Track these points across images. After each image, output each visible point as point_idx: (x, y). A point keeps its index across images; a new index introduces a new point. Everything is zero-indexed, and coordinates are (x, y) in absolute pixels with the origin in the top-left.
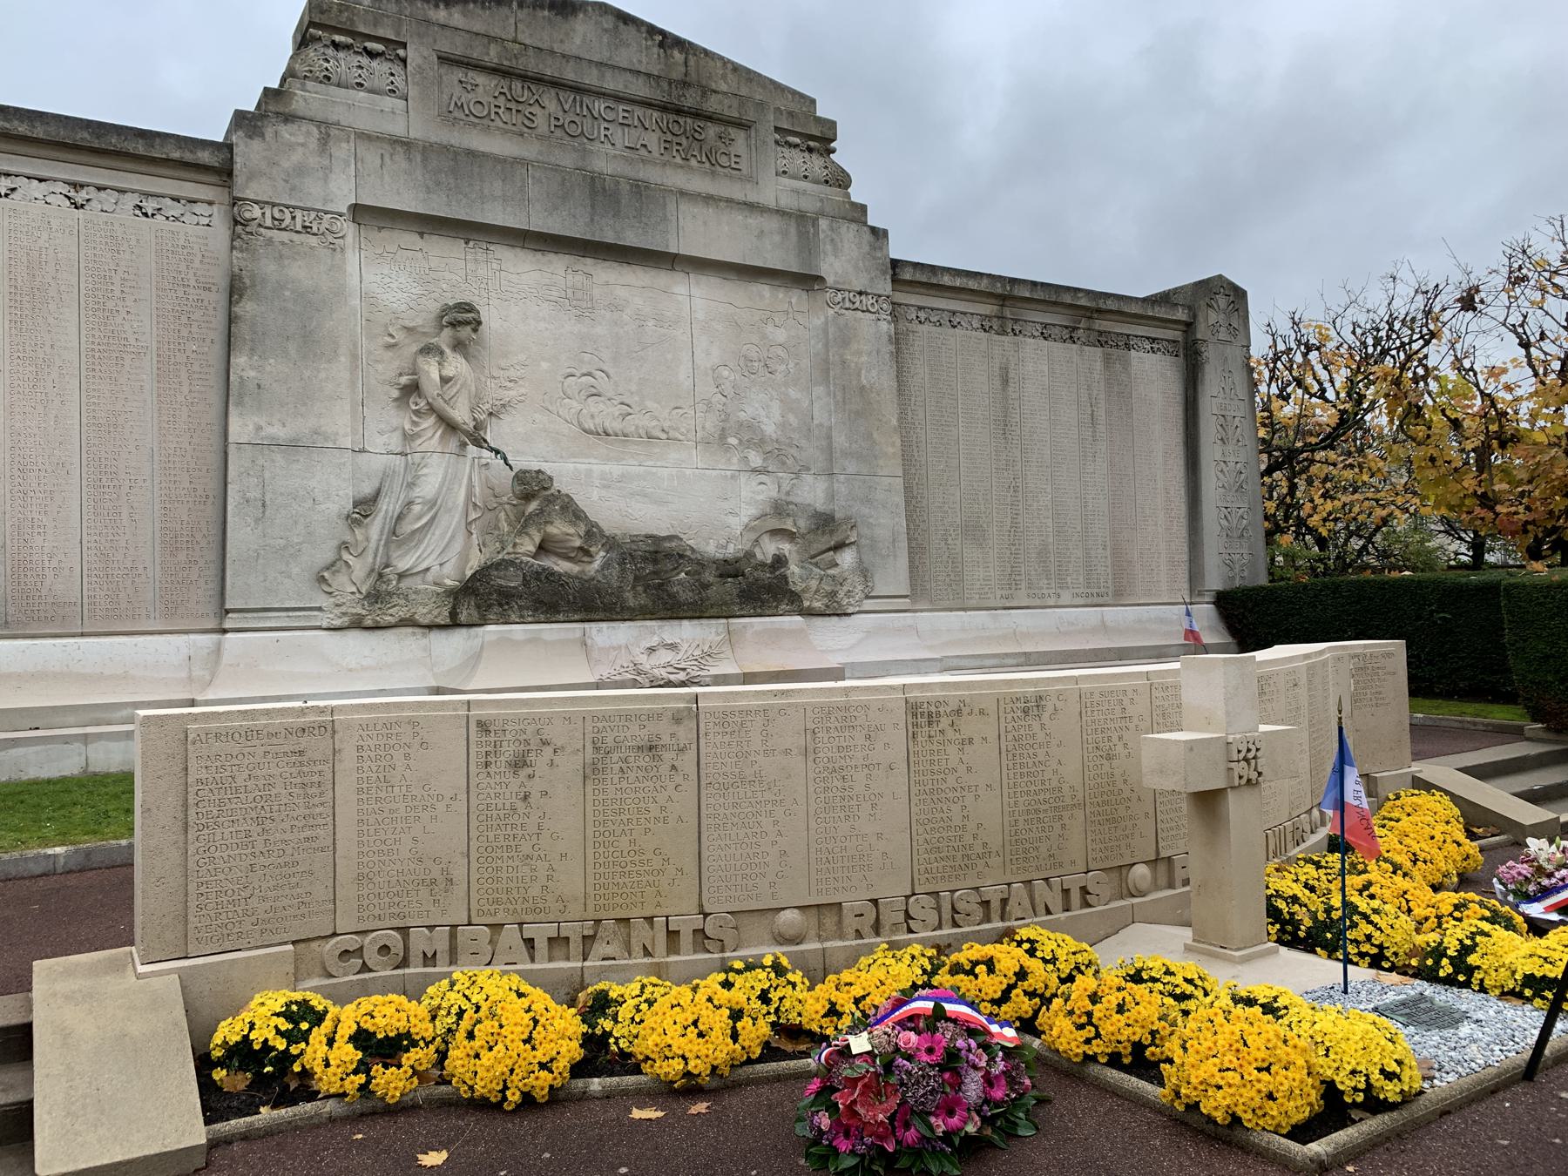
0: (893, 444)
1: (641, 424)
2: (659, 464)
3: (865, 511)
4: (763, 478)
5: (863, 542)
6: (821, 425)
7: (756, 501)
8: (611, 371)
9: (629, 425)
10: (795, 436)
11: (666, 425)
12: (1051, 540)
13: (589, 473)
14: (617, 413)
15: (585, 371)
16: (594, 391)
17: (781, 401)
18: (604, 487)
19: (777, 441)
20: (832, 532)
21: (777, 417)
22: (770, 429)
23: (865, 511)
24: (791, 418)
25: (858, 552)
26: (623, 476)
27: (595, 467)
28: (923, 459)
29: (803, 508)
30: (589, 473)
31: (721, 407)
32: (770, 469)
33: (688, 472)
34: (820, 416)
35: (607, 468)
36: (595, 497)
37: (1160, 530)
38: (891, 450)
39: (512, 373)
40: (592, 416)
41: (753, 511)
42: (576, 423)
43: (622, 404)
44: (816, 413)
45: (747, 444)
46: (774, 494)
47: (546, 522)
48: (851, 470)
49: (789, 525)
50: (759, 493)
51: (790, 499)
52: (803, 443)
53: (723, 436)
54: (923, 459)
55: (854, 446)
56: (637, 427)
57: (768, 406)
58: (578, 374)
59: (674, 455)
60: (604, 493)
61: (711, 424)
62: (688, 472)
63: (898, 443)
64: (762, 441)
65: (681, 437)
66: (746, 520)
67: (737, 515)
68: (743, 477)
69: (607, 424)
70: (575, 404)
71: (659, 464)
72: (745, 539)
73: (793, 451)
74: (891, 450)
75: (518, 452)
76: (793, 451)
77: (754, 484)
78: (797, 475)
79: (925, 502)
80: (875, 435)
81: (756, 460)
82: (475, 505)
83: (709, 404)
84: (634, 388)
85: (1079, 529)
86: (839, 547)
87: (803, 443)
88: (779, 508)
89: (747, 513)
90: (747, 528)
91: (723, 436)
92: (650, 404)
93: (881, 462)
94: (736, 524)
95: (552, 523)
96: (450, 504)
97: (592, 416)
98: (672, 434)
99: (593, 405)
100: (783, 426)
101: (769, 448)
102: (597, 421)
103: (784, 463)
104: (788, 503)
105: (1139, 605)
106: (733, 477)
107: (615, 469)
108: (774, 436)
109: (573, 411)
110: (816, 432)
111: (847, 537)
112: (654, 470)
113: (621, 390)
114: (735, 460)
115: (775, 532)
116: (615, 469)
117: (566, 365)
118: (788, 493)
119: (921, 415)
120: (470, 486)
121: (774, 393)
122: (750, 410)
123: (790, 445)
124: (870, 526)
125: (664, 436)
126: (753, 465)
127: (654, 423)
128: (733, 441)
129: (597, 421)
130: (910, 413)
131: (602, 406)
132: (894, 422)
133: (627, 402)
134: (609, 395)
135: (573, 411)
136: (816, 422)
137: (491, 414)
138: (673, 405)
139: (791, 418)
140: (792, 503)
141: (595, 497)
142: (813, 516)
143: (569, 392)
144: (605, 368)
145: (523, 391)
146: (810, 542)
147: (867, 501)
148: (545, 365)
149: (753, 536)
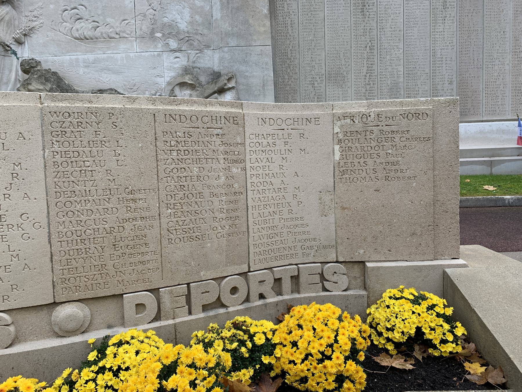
0: (264, 25)
1: (104, 31)
2: (115, 52)
3: (243, 68)
4: (177, 54)
5: (241, 87)
6: (216, 19)
7: (174, 68)
8: (86, 4)
9: (97, 33)
10: (200, 28)
11: (118, 30)
12: (401, 80)
13: (77, 60)
14: (91, 27)
15: (72, 6)
16: (78, 17)
17: (191, 8)
18: (86, 67)
19: (188, 32)
20: (216, 83)
21: (187, 17)
22: (183, 26)
23: (243, 68)
24: (197, 17)
25: (238, 94)
26: (95, 60)
27: (80, 57)
28: (296, 36)
29: (205, 70)
30: (77, 60)
31: (152, 17)
32: (183, 49)
33: (131, 55)
34: (217, 14)
35: (86, 57)
36: (81, 72)
37: (507, 67)
38: (262, 29)
39: (35, 13)
40: (77, 30)
41: (173, 74)
42: (69, 34)
43: (94, 21)
44: (214, 13)
45: (170, 35)
46: (185, 63)
47: (28, 84)
48: (232, 44)
49: (187, 79)
50: (175, 64)
51: (196, 65)
52: (206, 31)
53: (153, 32)
54: (296, 36)
55: (235, 29)
56: (102, 34)
57: (181, 13)
58: (69, 9)
59: (122, 46)
60: (86, 70)
61: (145, 27)
62: (131, 55)
63: (268, 23)
64: (178, 33)
65: (127, 36)
66: (168, 79)
67: (162, 77)
68: (165, 55)
69: (85, 33)
70: (68, 24)
71: (115, 52)
72: (166, 89)
73: (199, 37)
74: (262, 29)
75: (41, 53)
76: (199, 37)
77: (172, 58)
78: (201, 51)
79: (297, 61)
80: (251, 21)
81: (173, 44)
82: (19, 80)
83: (145, 16)
84: (100, 12)
85: (427, 71)
86: (221, 91)
87: (206, 31)
88: (186, 71)
89: (168, 75)
90: (169, 83)
91: (153, 32)
92: (109, 20)
93: (255, 37)
94: (162, 82)
95: (31, 84)
96: (5, 80)
97: (77, 30)
98: (122, 35)
99: (78, 25)
100: (191, 23)
101: (182, 37)
102: (80, 32)
103: (191, 45)
104: (193, 68)
105: (482, 121)
106: (159, 55)
107: (91, 57)
108: (186, 29)
109: (67, 28)
110: (214, 25)
111: (225, 84)
112: (112, 55)
113: (92, 14)
114: (160, 45)
115: (182, 85)
116: (91, 57)
117: (63, 5)
118: (194, 62)
119: (294, 6)
120: (17, 71)
121: (186, 4)
122: (170, 16)
123: (196, 34)
124: (246, 77)
125: (118, 36)
126: (172, 48)
127: (111, 30)
128: (159, 35)
129: (80, 32)
130: (286, 6)
131: (83, 24)
132: (266, 11)
133: (97, 20)
134: (87, 18)
135: (67, 28)
136: (214, 18)
137: (25, 35)
138: (122, 18)
139: (197, 17)
140: (197, 67)
141: (81, 72)
142: (211, 74)
143: (65, 19)
144: (83, 4)
145: (41, 21)
146: (205, 89)
147: (245, 62)
148: (52, 6)
149: (170, 88)
